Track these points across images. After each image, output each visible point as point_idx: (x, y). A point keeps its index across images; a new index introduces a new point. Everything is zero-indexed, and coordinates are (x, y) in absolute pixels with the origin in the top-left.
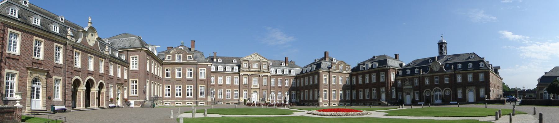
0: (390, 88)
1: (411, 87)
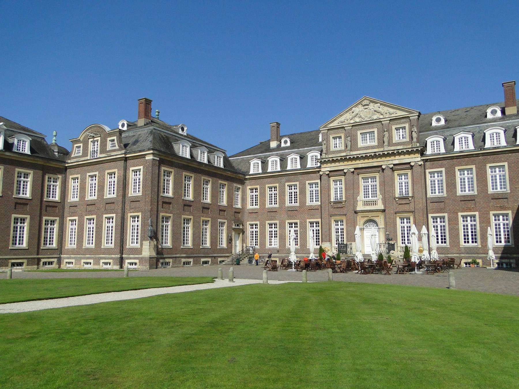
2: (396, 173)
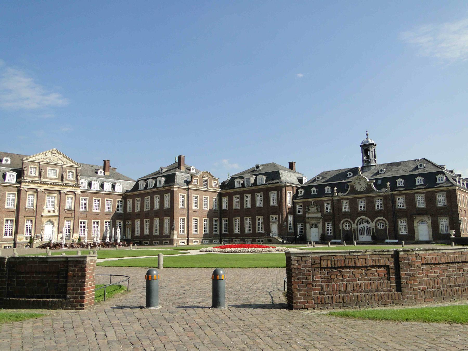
0: (285, 216)
1: (320, 215)
2: (67, 196)
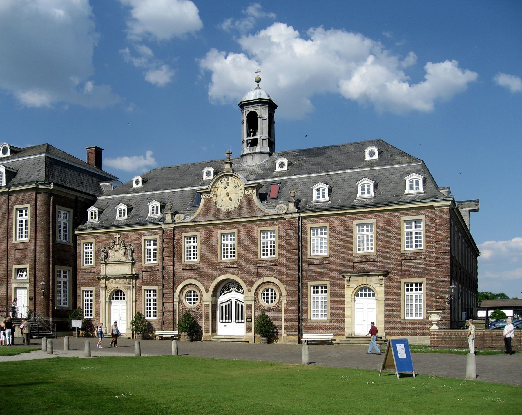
1: (127, 269)
